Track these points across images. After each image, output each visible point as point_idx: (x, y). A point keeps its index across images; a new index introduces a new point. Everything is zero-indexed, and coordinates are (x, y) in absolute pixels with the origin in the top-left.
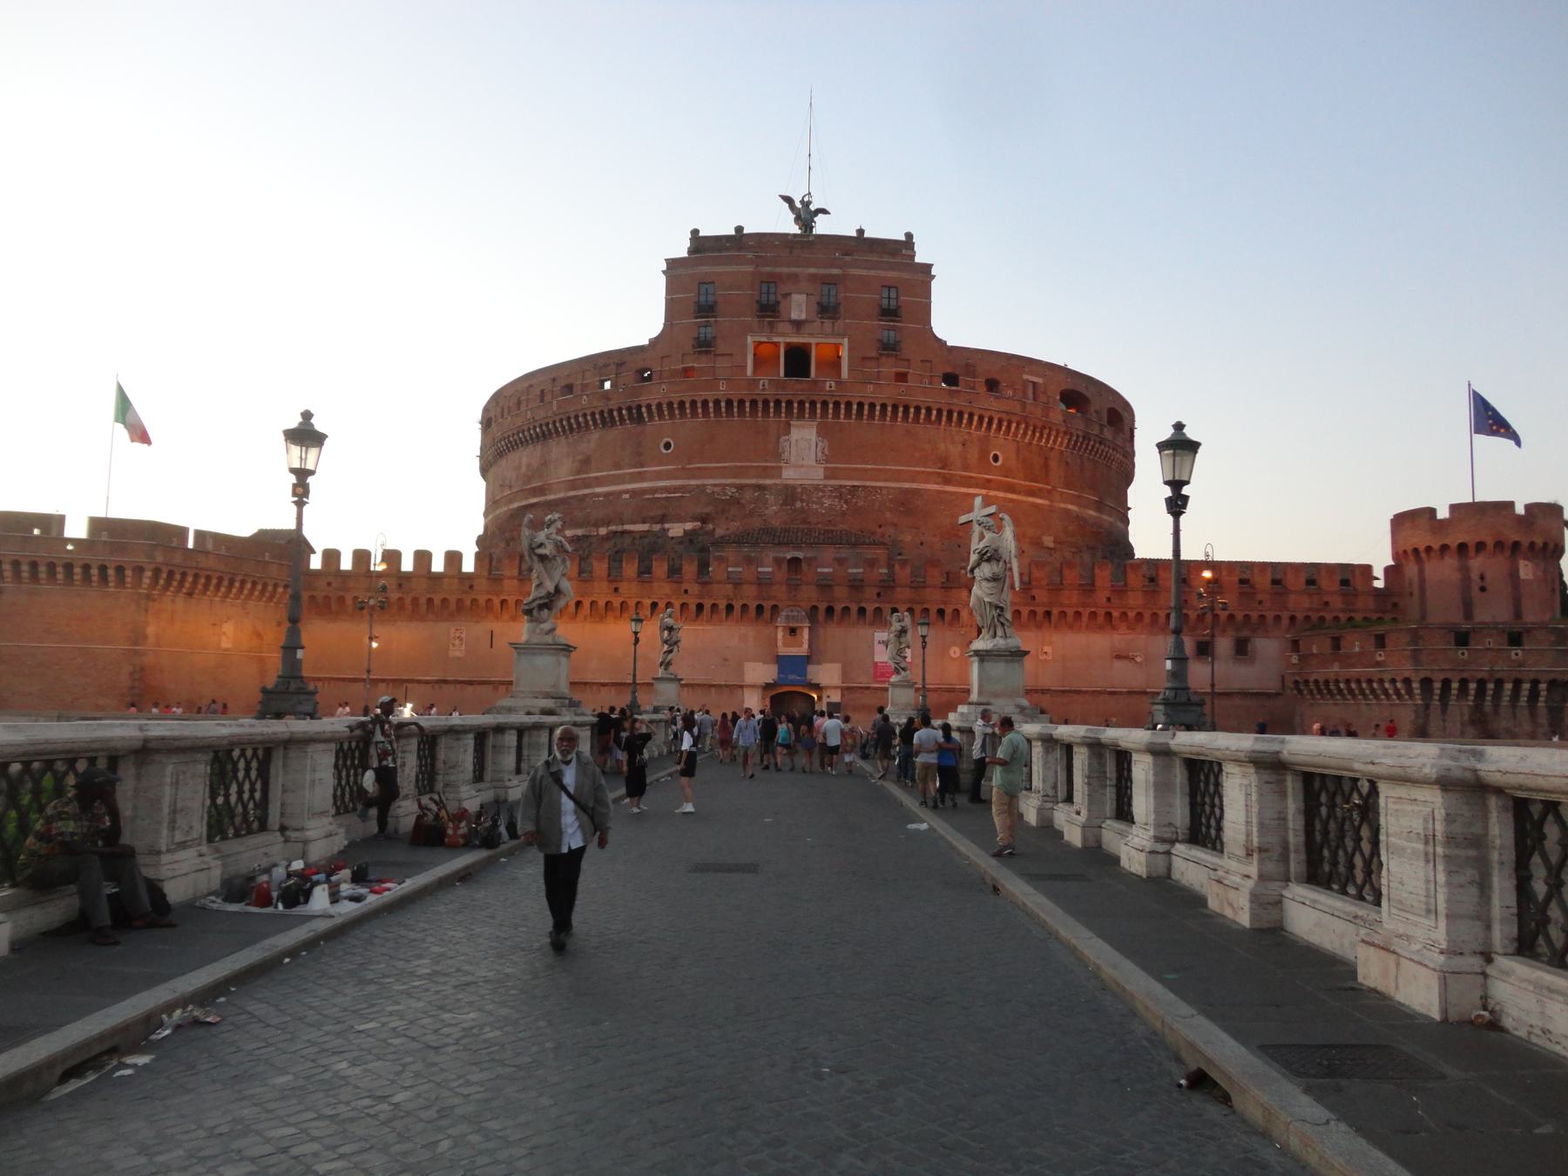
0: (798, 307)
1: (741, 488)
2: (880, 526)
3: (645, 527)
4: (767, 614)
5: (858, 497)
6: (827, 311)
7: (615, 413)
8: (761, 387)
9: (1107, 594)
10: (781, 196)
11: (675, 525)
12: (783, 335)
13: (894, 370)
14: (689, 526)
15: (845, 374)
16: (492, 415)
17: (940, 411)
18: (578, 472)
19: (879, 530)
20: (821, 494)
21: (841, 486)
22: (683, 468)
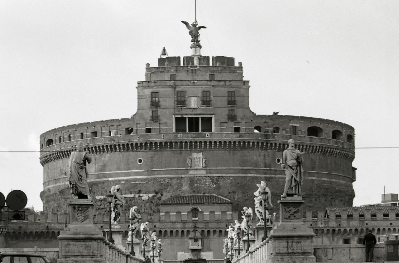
0: (194, 102)
1: (171, 179)
2: (230, 193)
3: (132, 196)
4: (185, 233)
5: (220, 181)
6: (206, 102)
7: (117, 147)
8: (179, 137)
9: (311, 223)
10: (182, 21)
11: (145, 195)
12: (186, 115)
13: (234, 127)
14: (151, 195)
15: (213, 130)
16: (51, 137)
17: (253, 143)
18: (101, 171)
19: (230, 194)
20: (205, 181)
21: (213, 177)
22: (148, 171)
